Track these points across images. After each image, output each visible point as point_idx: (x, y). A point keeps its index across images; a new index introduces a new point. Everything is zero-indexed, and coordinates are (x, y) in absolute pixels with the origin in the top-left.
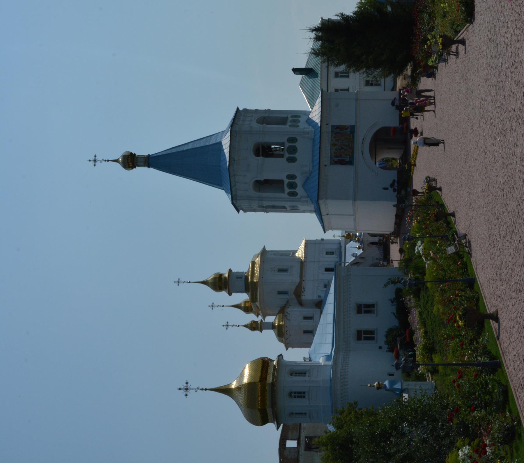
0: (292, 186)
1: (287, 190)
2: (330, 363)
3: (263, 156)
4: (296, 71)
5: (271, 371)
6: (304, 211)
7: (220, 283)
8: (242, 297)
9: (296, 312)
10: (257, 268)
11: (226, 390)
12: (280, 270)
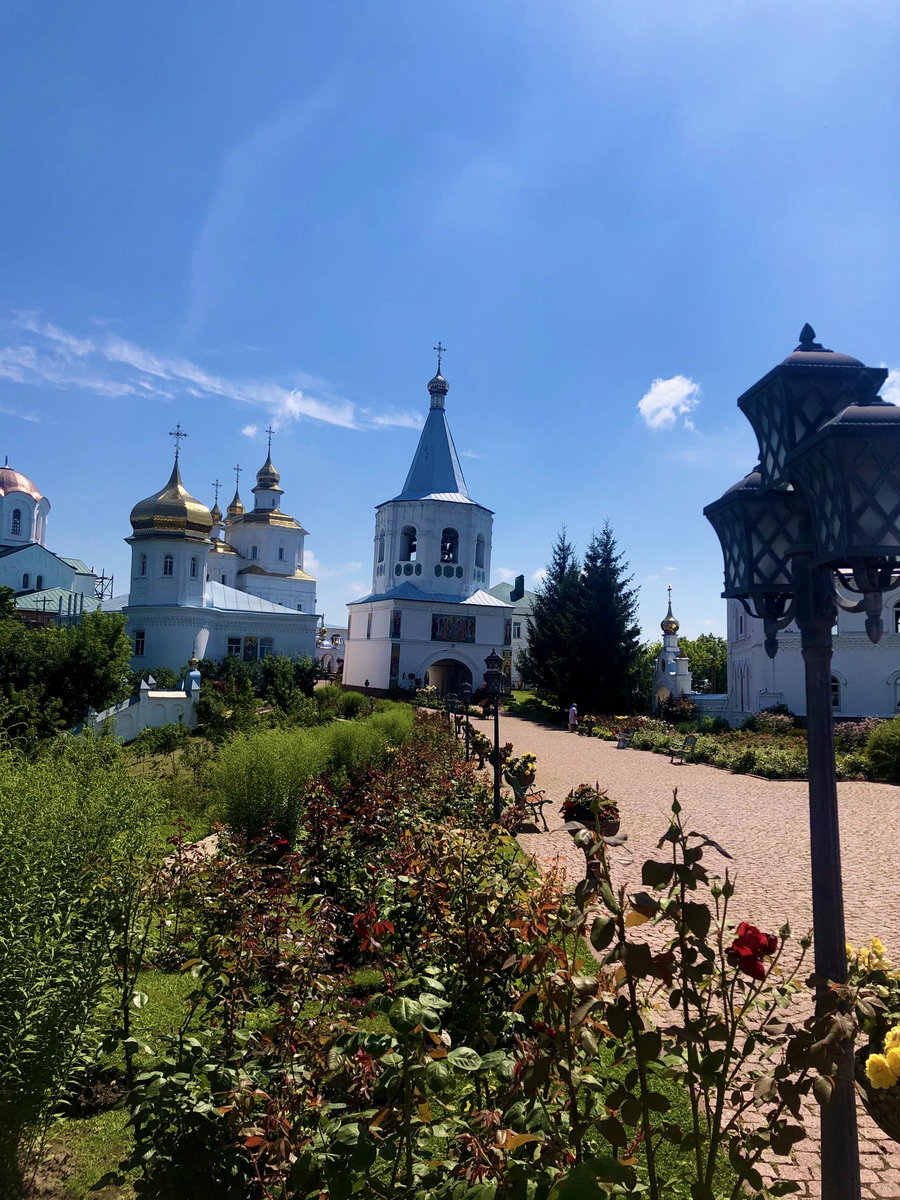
0: (408, 570)
1: (403, 564)
2: (204, 606)
4: (520, 580)
5: (199, 534)
6: (375, 582)
7: (266, 480)
8: (248, 505)
9: (232, 567)
10: (287, 524)
11: (174, 480)
12: (281, 550)
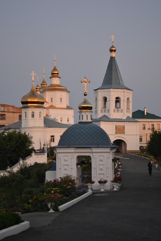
1: (103, 109)
3: (116, 100)
